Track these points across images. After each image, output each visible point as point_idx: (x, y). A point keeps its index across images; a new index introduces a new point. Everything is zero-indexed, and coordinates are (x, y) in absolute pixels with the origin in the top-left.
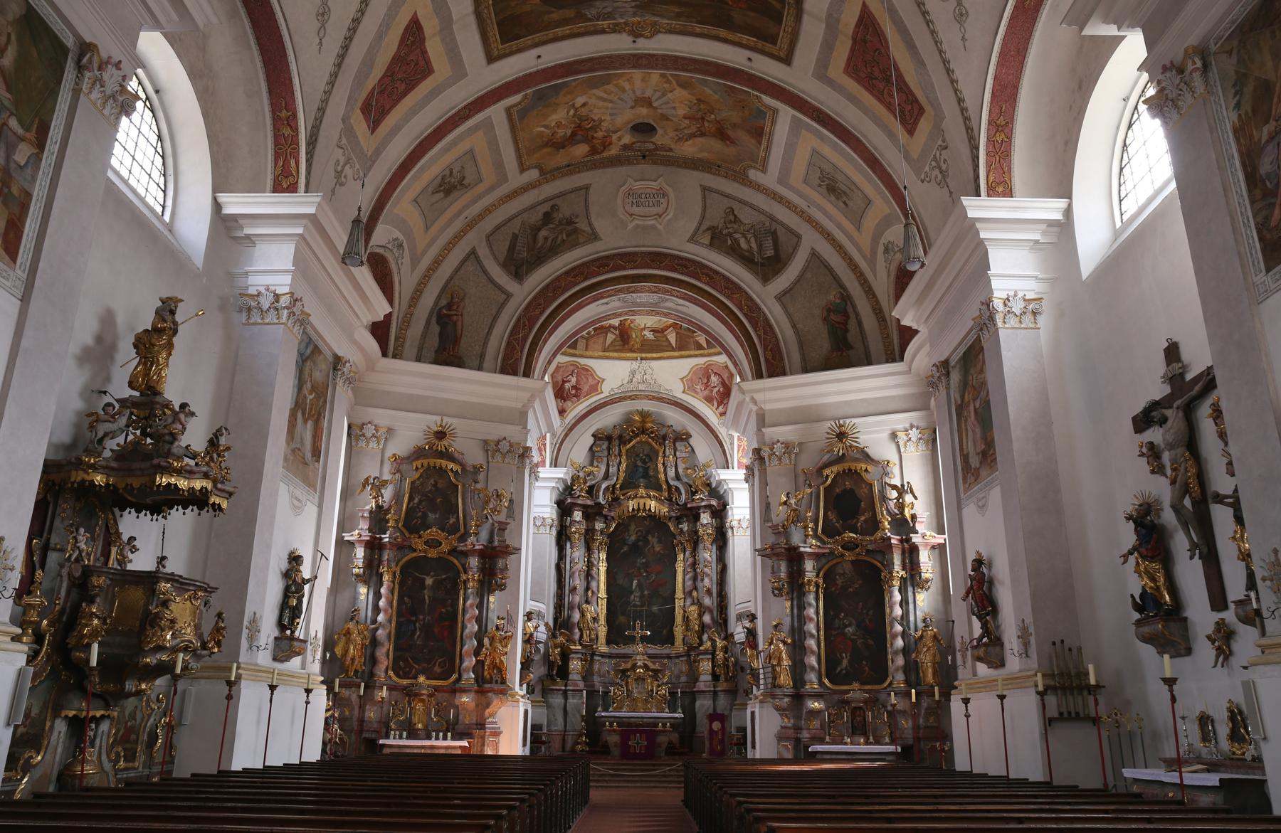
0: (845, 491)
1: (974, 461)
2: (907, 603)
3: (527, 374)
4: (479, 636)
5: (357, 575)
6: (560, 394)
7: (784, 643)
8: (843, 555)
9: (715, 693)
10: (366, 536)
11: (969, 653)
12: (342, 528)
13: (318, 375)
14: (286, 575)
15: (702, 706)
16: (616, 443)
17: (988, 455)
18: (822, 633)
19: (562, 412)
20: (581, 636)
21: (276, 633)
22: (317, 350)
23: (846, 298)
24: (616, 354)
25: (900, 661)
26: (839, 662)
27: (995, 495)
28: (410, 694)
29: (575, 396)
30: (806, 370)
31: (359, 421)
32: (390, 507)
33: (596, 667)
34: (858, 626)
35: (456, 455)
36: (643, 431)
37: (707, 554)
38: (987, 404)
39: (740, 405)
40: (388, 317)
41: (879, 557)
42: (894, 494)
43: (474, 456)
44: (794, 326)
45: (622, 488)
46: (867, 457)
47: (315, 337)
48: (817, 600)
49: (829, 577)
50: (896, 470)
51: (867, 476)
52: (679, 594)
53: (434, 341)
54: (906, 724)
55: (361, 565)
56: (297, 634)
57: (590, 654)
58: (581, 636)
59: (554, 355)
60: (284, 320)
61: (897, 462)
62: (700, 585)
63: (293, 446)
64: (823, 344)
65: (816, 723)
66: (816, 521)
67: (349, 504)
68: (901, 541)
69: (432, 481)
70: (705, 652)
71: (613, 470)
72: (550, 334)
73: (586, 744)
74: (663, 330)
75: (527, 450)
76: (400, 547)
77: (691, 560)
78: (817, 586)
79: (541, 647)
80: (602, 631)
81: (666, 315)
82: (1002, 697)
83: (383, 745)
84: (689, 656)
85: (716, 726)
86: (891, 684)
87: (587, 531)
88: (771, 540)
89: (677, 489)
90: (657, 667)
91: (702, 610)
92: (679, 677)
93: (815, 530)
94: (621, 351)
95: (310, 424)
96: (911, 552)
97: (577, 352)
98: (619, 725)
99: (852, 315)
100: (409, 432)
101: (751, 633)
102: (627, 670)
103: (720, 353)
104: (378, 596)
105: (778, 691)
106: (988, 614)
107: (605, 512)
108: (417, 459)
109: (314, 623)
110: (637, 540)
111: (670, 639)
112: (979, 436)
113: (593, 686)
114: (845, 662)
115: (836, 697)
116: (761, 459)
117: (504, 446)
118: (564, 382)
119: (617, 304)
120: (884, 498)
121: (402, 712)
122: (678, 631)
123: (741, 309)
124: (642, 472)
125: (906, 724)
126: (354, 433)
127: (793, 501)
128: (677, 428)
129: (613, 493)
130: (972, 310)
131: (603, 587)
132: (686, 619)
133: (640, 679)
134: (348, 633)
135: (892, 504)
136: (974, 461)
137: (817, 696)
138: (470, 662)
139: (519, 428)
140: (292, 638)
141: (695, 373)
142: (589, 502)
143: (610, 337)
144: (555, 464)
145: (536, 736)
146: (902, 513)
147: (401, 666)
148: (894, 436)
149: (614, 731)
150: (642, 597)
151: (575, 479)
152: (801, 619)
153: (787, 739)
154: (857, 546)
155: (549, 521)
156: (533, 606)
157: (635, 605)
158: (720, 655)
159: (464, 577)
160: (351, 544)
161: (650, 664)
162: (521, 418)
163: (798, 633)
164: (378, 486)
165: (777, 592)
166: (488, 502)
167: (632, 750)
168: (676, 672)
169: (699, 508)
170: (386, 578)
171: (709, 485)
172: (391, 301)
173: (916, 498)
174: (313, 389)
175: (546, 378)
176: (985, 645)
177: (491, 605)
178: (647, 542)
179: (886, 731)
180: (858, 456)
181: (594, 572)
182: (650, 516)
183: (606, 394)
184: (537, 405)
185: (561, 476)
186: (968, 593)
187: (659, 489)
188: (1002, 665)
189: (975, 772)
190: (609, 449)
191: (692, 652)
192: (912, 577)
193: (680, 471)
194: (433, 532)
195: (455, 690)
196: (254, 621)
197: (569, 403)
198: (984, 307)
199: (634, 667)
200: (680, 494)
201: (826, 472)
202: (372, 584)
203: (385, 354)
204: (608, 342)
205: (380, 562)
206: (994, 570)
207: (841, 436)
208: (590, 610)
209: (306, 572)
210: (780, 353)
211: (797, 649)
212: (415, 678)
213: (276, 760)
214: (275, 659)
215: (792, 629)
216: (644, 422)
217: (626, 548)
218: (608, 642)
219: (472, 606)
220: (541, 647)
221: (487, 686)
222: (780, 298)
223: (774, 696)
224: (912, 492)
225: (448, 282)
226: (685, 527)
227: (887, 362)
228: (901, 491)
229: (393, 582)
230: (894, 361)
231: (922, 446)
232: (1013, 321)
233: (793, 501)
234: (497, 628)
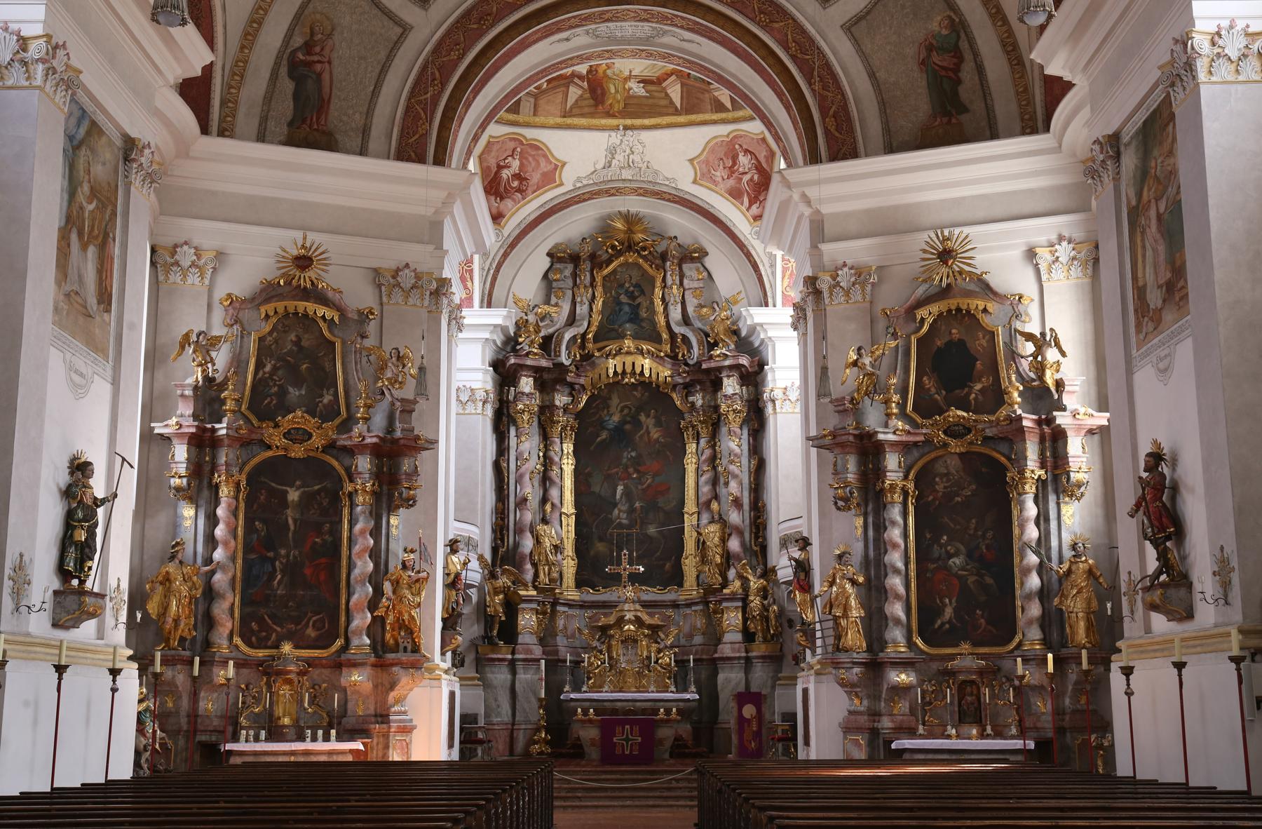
0: (950, 344)
1: (1154, 298)
2: (1047, 520)
3: (440, 160)
4: (376, 580)
5: (178, 489)
6: (494, 188)
7: (853, 582)
8: (945, 445)
9: (748, 660)
10: (190, 427)
11: (1139, 598)
12: (149, 413)
13: (99, 171)
14: (68, 493)
15: (728, 680)
16: (586, 266)
17: (1176, 288)
18: (913, 566)
19: (497, 218)
20: (536, 575)
21: (56, 584)
22: (95, 129)
23: (958, 26)
24: (583, 121)
25: (1035, 610)
26: (940, 612)
27: (1185, 352)
28: (269, 671)
29: (519, 190)
30: (890, 149)
31: (168, 241)
32: (226, 379)
33: (560, 623)
34: (969, 555)
35: (330, 294)
36: (630, 246)
37: (734, 443)
38: (1176, 208)
39: (784, 206)
40: (208, 69)
41: (1004, 447)
42: (1030, 348)
43: (359, 295)
44: (872, 75)
45: (596, 339)
46: (987, 290)
47: (90, 107)
48: (905, 514)
49: (924, 479)
50: (1034, 310)
51: (986, 320)
52: (690, 506)
53: (285, 107)
54: (1042, 706)
55: (183, 471)
56: (89, 585)
57: (550, 603)
58: (536, 575)
59: (483, 126)
60: (38, 81)
61: (1035, 295)
62: (722, 491)
63: (68, 288)
64: (919, 105)
65: (903, 706)
66: (904, 392)
67: (159, 375)
68: (1039, 422)
69: (293, 337)
70: (732, 597)
71: (582, 310)
72: (476, 92)
73: (546, 742)
74: (660, 81)
75: (444, 283)
76: (244, 443)
77: (708, 453)
78: (905, 493)
79: (473, 593)
80: (569, 566)
81: (664, 57)
82: (1180, 666)
83: (230, 753)
84: (707, 603)
85: (749, 711)
86: (1020, 644)
87: (542, 409)
88: (833, 421)
89: (685, 339)
90: (655, 621)
91: (727, 530)
92: (690, 636)
93: (902, 406)
94: (592, 115)
95: (92, 251)
96: (1055, 440)
97: (520, 118)
98: (597, 712)
99: (968, 56)
100: (252, 258)
101: (802, 568)
102: (609, 627)
103: (752, 119)
104: (212, 520)
105: (843, 657)
106: (1168, 538)
107: (570, 378)
108: (267, 300)
109: (115, 567)
110: (623, 422)
111: (676, 578)
112: (1162, 257)
113: (557, 652)
114: (949, 612)
115: (935, 666)
116: (817, 293)
117: (407, 279)
118: (500, 168)
120: (1013, 355)
121: (257, 700)
122: (690, 565)
123: (786, 48)
124: (628, 314)
125: (1042, 706)
126: (163, 259)
127: (867, 360)
128: (684, 240)
129: (583, 346)
130: (1160, 52)
131: (569, 496)
132: (701, 545)
133: (630, 641)
134: (167, 580)
135: (1025, 365)
136: (1154, 298)
137: (904, 664)
138: (362, 620)
139: (431, 248)
140: (81, 592)
141: (713, 150)
142: (544, 363)
143: (574, 93)
144: (488, 302)
145: (468, 731)
146: (1041, 377)
147: (254, 627)
148: (1031, 254)
149: (590, 721)
150: (631, 511)
151: (521, 325)
152: (879, 545)
153: (858, 730)
154: (969, 431)
155: (480, 395)
156: (459, 529)
157: (620, 526)
158: (755, 602)
159: (349, 488)
160: (166, 439)
161: (645, 617)
162: (432, 233)
163: (875, 568)
164: (205, 345)
165: (843, 503)
166: (383, 368)
167: (618, 751)
168: (686, 629)
169: (719, 369)
170: (224, 492)
171: (736, 333)
172: (210, 42)
173: (1063, 354)
174: (94, 194)
175: (472, 166)
176: (1162, 585)
177: (394, 531)
178: (637, 424)
179: (1011, 717)
180: (972, 287)
181: (554, 474)
182: (642, 383)
183: (568, 187)
184: (457, 209)
185: (499, 321)
186: (1138, 506)
187: (655, 338)
188: (1189, 615)
189: (1138, 777)
190: (575, 275)
191: (711, 597)
192: (1056, 478)
193: (690, 310)
194: (297, 418)
195: (338, 665)
196: (20, 567)
197: (508, 203)
198: (1179, 48)
199: (621, 621)
200: (690, 347)
201: (922, 313)
202: (202, 502)
203: (205, 130)
205: (214, 468)
206: (1179, 470)
207: (946, 255)
208: (550, 534)
209: (98, 487)
210: (849, 119)
211: (874, 591)
212: (277, 647)
213: (70, 778)
214: (55, 625)
215: (866, 563)
216: (630, 231)
217: (604, 435)
218: (580, 584)
219: (362, 532)
220: (473, 593)
221: (391, 656)
222: (850, 28)
223: (837, 665)
224: (1058, 345)
225: (303, 8)
226: (698, 399)
227: (1023, 133)
228: (1040, 343)
229: (237, 498)
230: (1034, 131)
231: (1076, 271)
232: (1224, 71)
233: (867, 360)
234: (404, 567)
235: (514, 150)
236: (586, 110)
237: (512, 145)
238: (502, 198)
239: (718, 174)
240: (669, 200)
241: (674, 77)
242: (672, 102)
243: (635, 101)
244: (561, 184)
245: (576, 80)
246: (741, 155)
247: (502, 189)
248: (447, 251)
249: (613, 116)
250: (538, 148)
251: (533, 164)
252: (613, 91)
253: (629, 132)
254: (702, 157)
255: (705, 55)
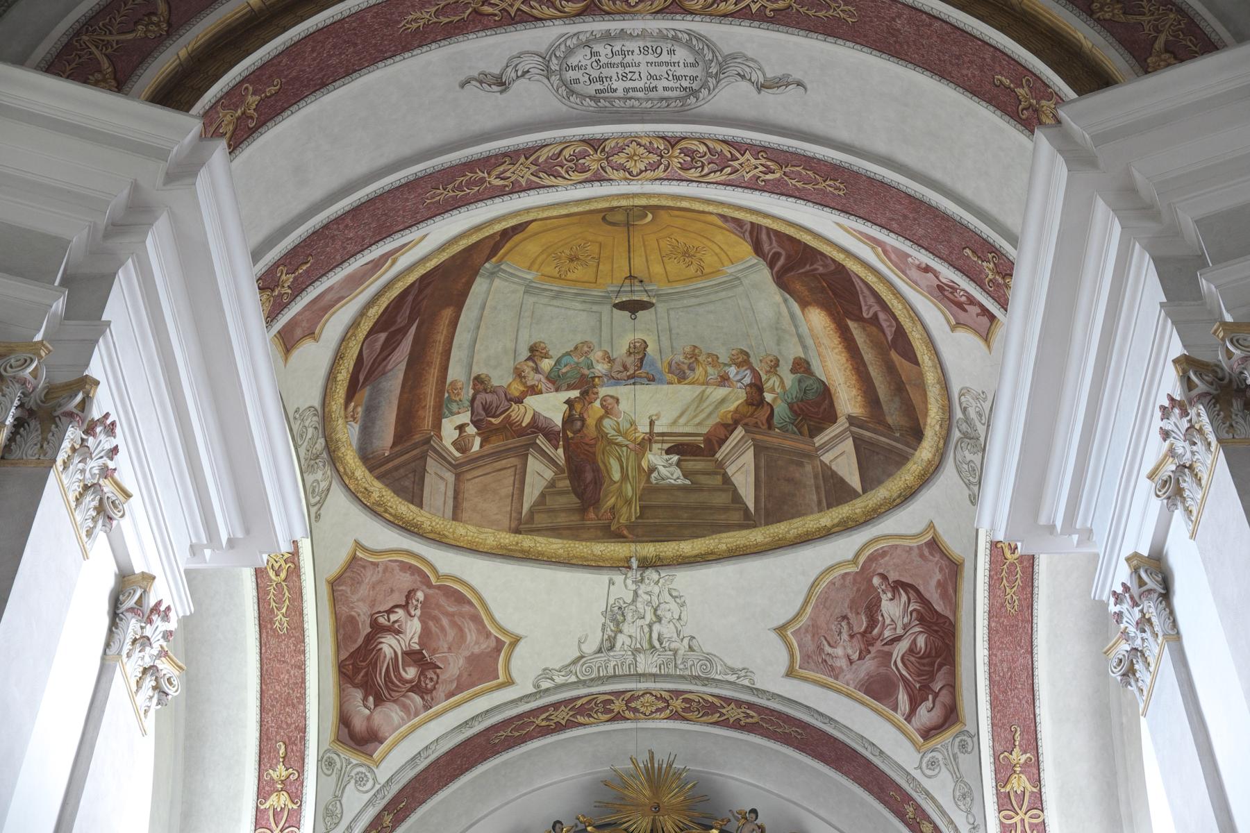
24: (555, 545)
29: (417, 688)
74: (713, 442)
94: (572, 532)
118: (378, 629)
119: (533, 97)
141: (824, 601)
143: (539, 474)
183: (524, 686)
184: (156, 245)
204: (531, 494)
235: (410, 595)
236: (562, 519)
237: (405, 581)
238: (379, 700)
239: (839, 651)
240: (737, 726)
241: (739, 432)
242: (737, 498)
243: (662, 499)
244: (510, 682)
245: (541, 441)
246: (885, 598)
247: (380, 680)
248: (108, 323)
249: (618, 536)
250: (460, 599)
251: (451, 633)
252: (616, 476)
253: (652, 574)
254: (805, 619)
255: (817, 125)
